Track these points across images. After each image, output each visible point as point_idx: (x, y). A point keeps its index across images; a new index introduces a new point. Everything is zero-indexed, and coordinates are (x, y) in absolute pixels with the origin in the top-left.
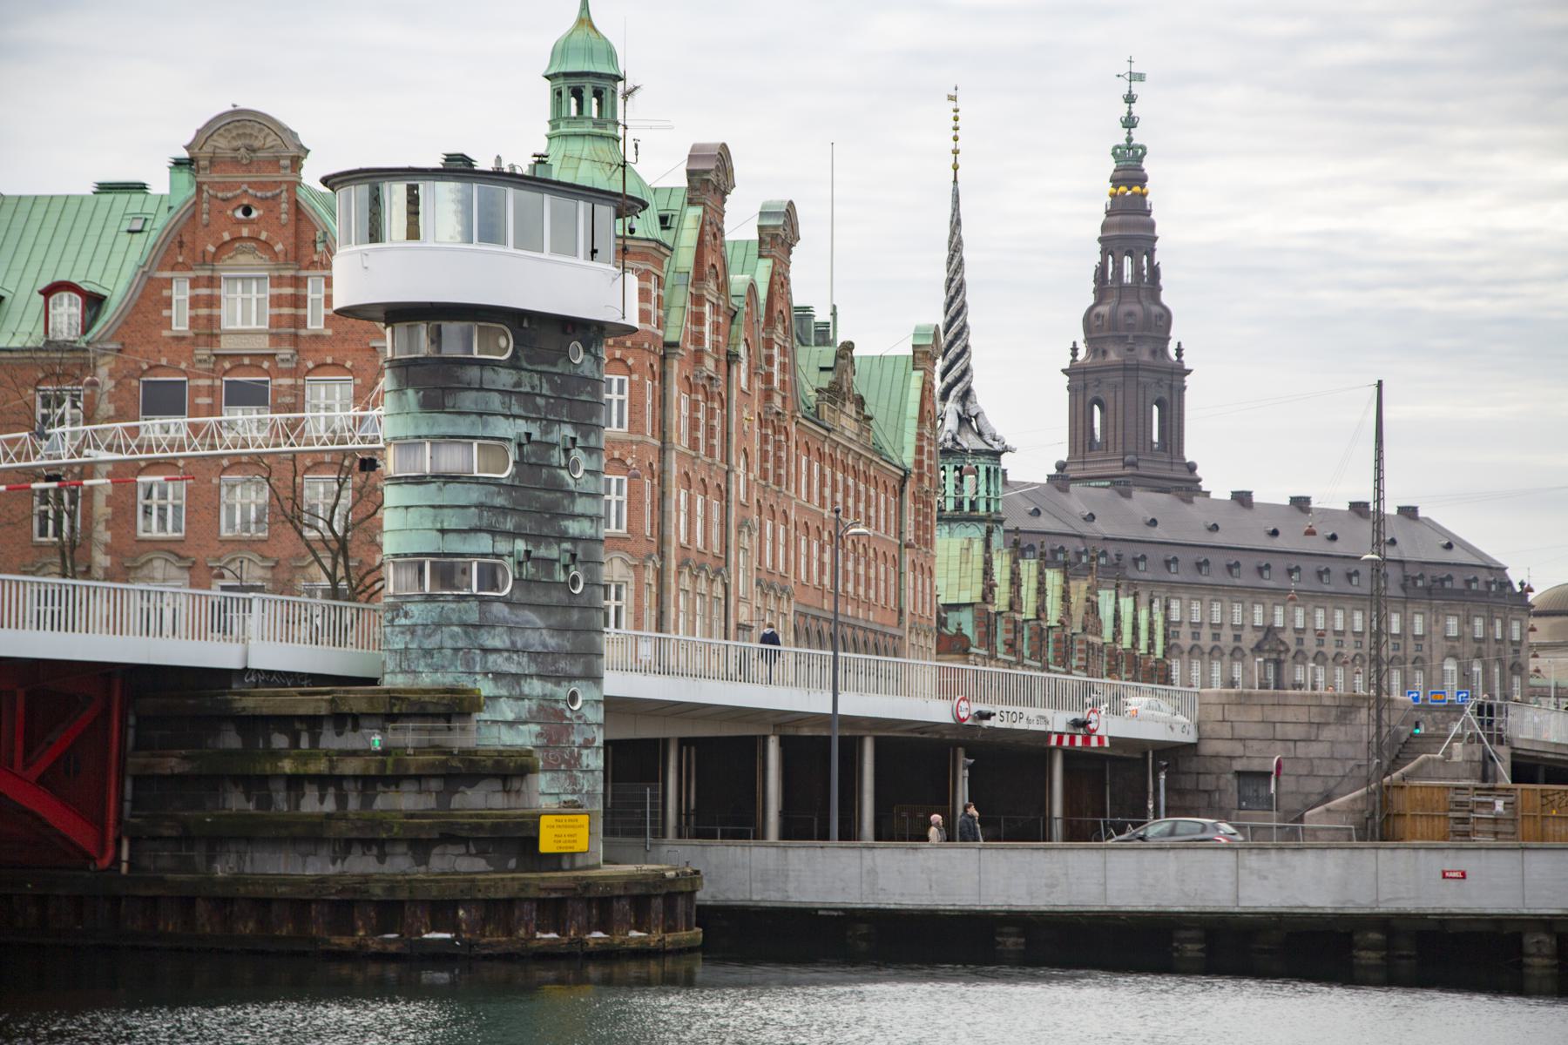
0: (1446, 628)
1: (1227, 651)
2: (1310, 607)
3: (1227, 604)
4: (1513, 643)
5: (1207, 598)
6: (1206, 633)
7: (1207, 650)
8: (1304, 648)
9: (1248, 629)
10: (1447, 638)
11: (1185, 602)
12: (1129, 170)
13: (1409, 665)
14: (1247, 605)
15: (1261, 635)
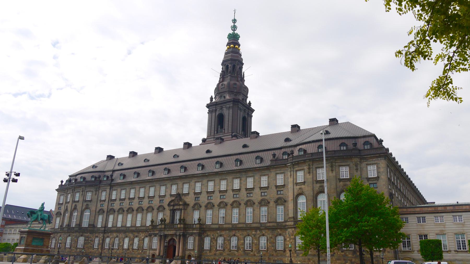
0: (295, 179)
1: (156, 208)
2: (205, 181)
3: (158, 186)
4: (369, 179)
5: (148, 186)
6: (146, 200)
7: (145, 208)
8: (200, 202)
9: (168, 196)
10: (297, 184)
11: (137, 189)
12: (234, 40)
13: (272, 204)
14: (169, 186)
15: (173, 198)
